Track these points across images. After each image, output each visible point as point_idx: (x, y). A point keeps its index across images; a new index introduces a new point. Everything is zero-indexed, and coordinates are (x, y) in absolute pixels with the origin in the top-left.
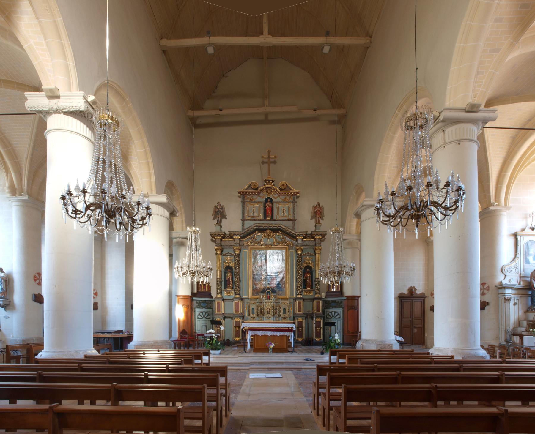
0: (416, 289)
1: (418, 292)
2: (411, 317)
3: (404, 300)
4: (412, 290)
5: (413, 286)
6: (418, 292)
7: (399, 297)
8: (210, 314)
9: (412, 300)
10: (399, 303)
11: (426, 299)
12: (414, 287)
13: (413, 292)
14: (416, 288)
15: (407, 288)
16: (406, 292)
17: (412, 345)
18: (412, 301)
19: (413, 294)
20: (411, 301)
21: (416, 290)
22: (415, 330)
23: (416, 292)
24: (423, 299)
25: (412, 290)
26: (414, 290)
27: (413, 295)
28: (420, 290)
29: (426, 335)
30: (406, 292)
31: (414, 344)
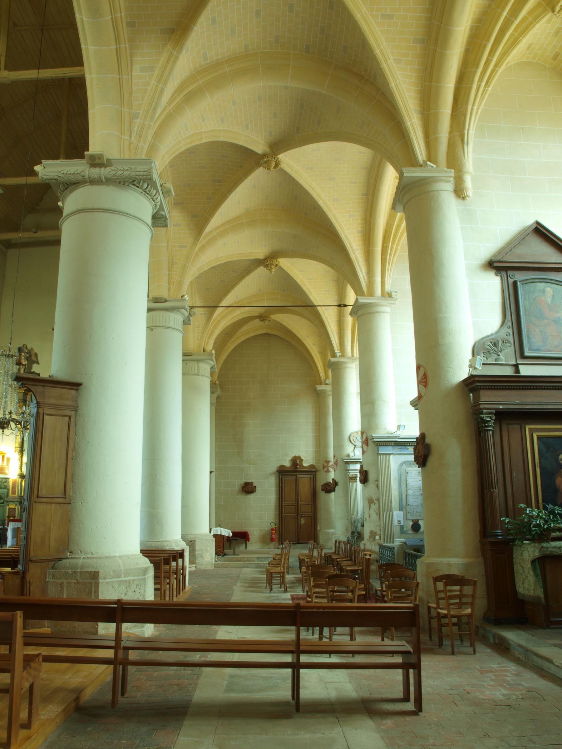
0: (303, 460)
1: (305, 464)
2: (295, 502)
3: (286, 476)
4: (296, 461)
5: (297, 455)
6: (305, 464)
7: (277, 471)
8: (3, 497)
9: (296, 475)
10: (278, 481)
11: (318, 474)
12: (299, 457)
13: (297, 465)
14: (303, 458)
15: (290, 458)
16: (288, 464)
17: (298, 543)
18: (297, 477)
19: (297, 467)
20: (295, 477)
21: (301, 460)
22: (303, 521)
23: (302, 464)
24: (313, 474)
25: (296, 461)
26: (298, 460)
27: (297, 468)
28: (308, 461)
29: (319, 528)
30: (288, 464)
31: (301, 542)
